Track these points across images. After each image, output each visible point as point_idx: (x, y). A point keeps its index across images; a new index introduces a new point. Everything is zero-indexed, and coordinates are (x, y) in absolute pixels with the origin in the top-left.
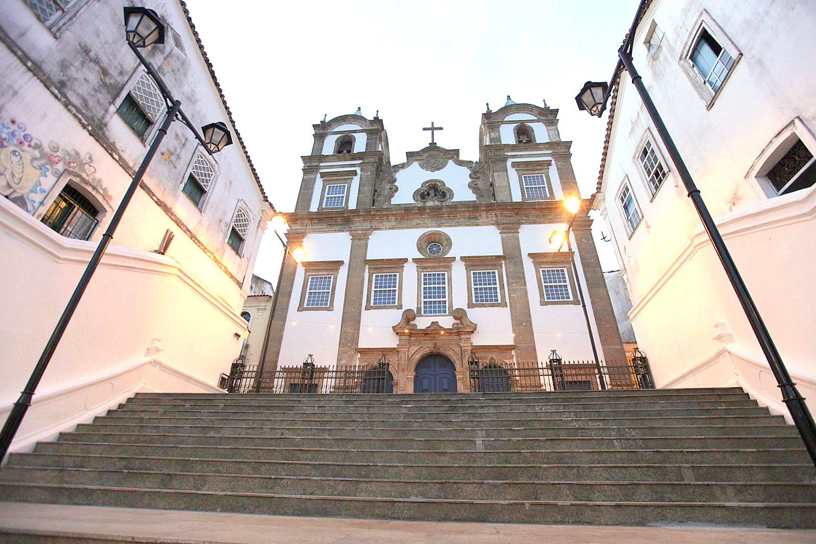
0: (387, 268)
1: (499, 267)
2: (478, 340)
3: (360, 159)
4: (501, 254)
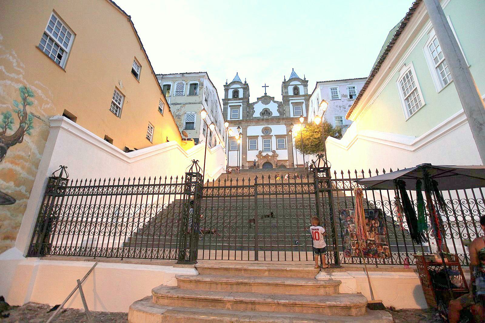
2: (278, 159)
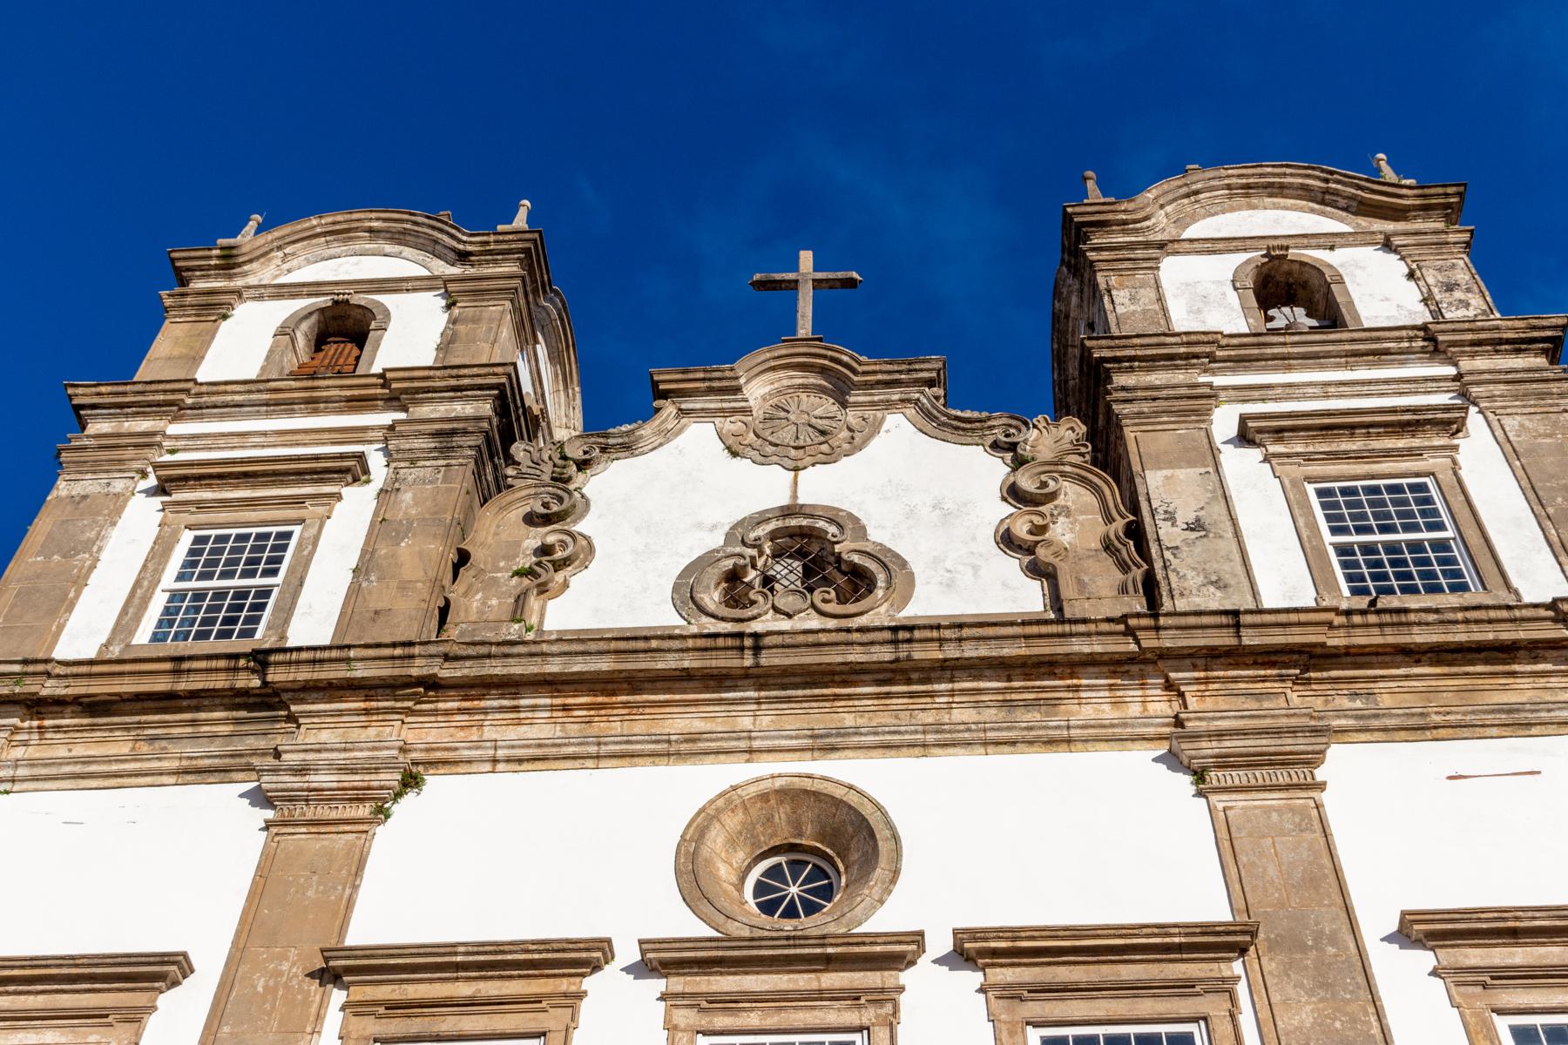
0: (471, 1003)
1: (1214, 1006)
3: (394, 400)
4: (1215, 908)
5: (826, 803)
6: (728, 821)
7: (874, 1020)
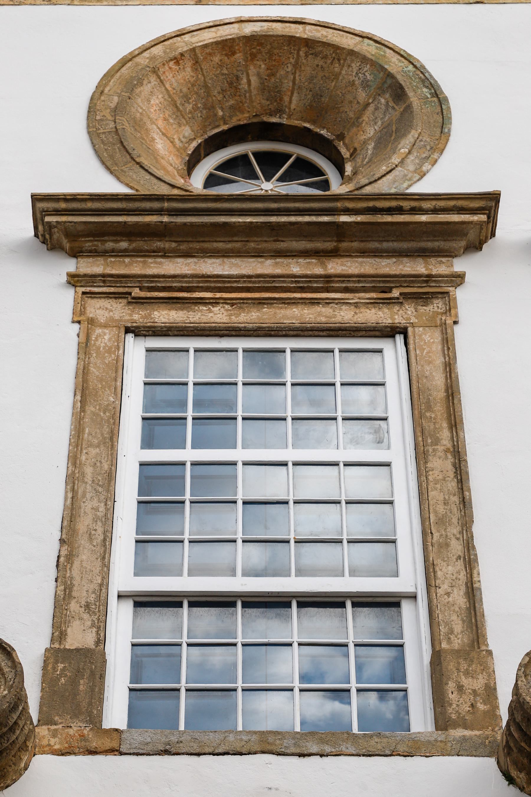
5: (325, 57)
6: (170, 76)
7: (413, 320)
